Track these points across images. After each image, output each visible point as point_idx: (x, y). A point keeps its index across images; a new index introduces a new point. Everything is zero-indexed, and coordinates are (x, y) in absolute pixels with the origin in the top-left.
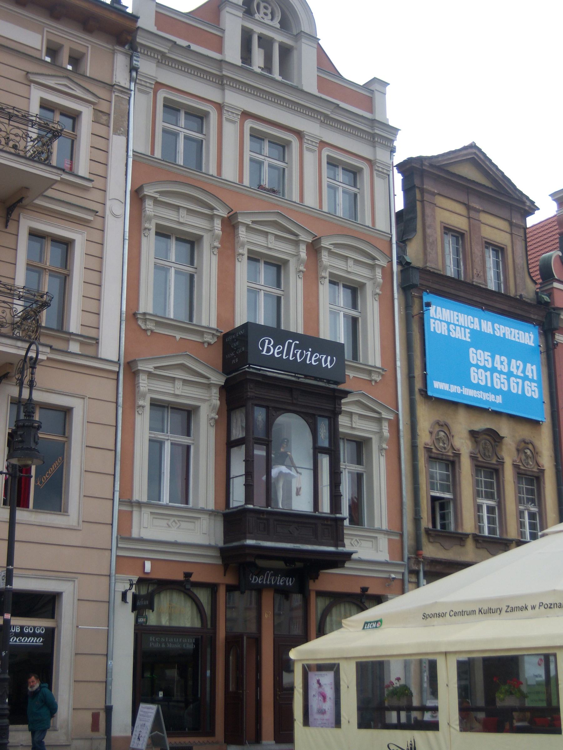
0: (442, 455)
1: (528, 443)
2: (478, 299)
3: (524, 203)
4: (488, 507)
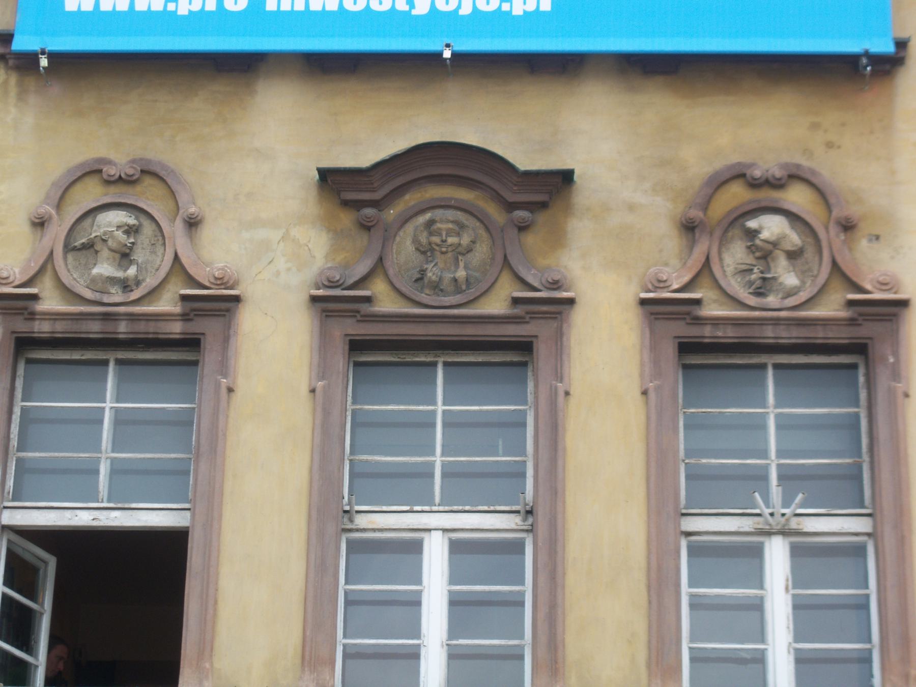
0: (107, 317)
4: (461, 548)
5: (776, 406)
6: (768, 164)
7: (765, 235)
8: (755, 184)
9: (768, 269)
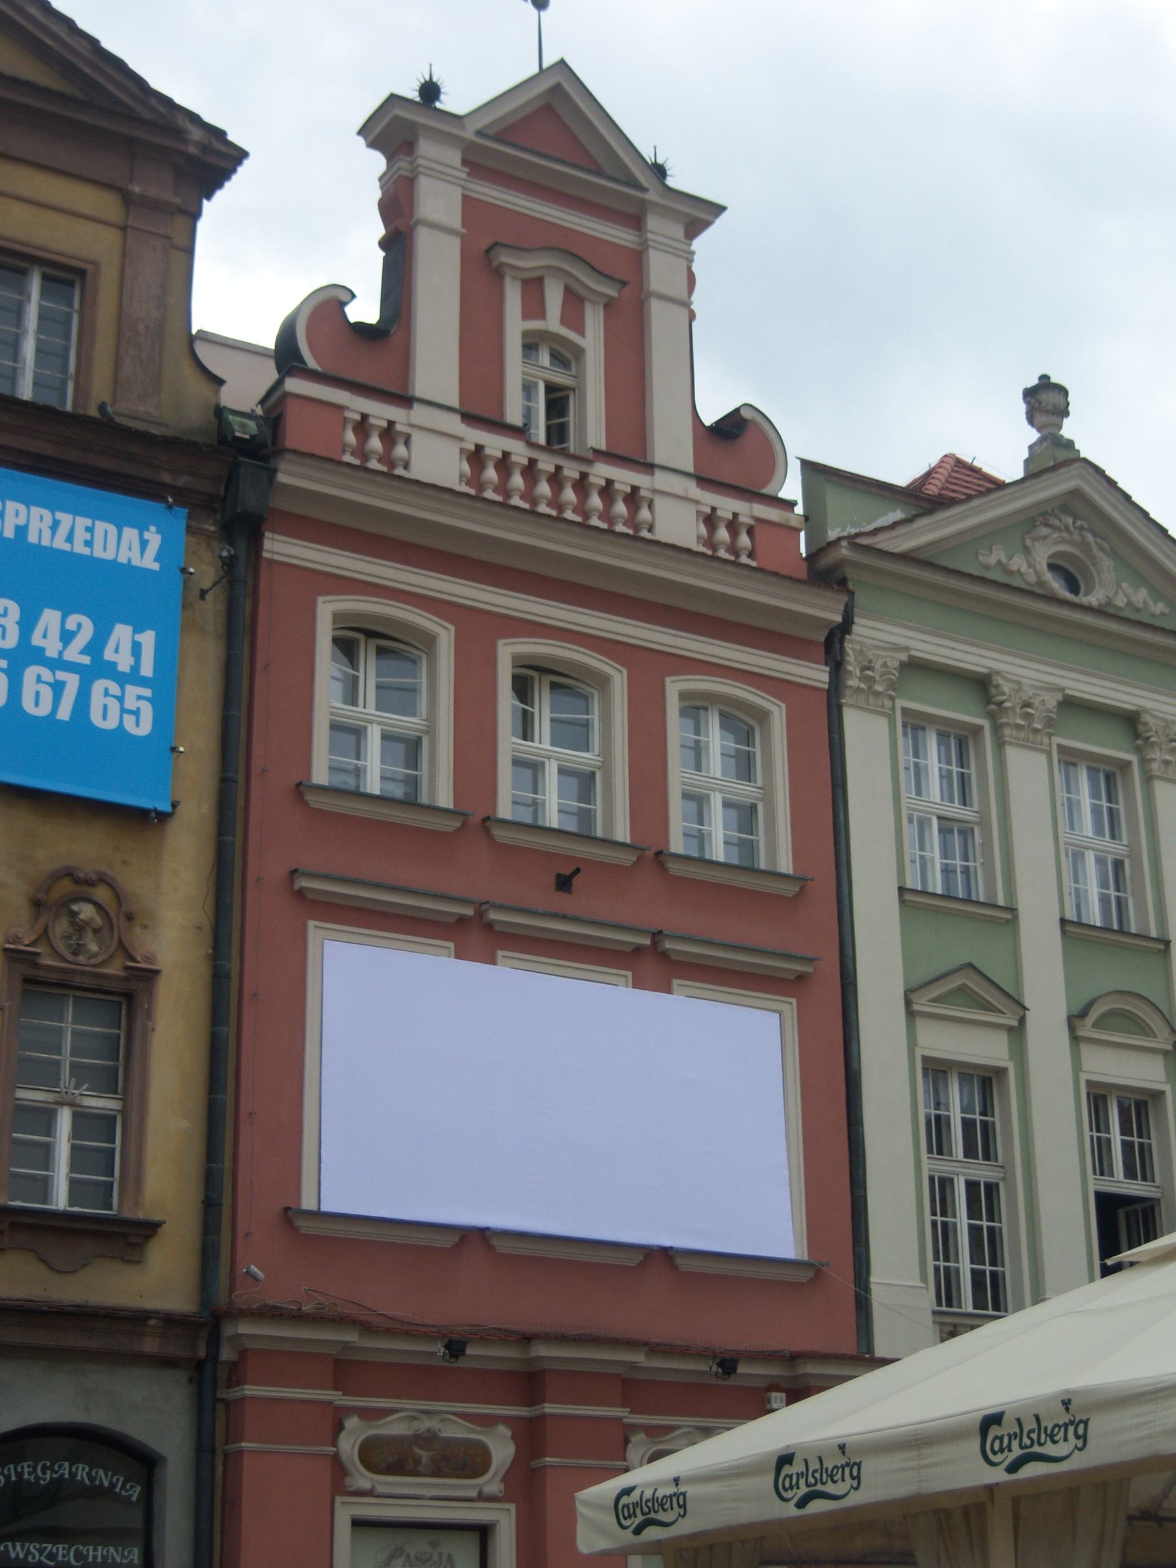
1: (90, 883)
3: (179, 134)
5: (74, 1022)
6: (87, 870)
7: (82, 916)
8: (78, 882)
9: (80, 938)
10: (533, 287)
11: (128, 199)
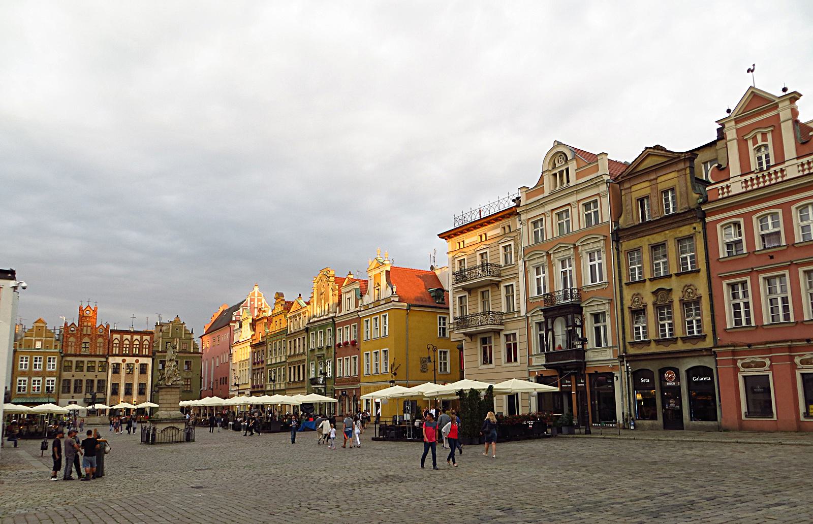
2: (653, 227)
10: (754, 139)
11: (678, 171)
